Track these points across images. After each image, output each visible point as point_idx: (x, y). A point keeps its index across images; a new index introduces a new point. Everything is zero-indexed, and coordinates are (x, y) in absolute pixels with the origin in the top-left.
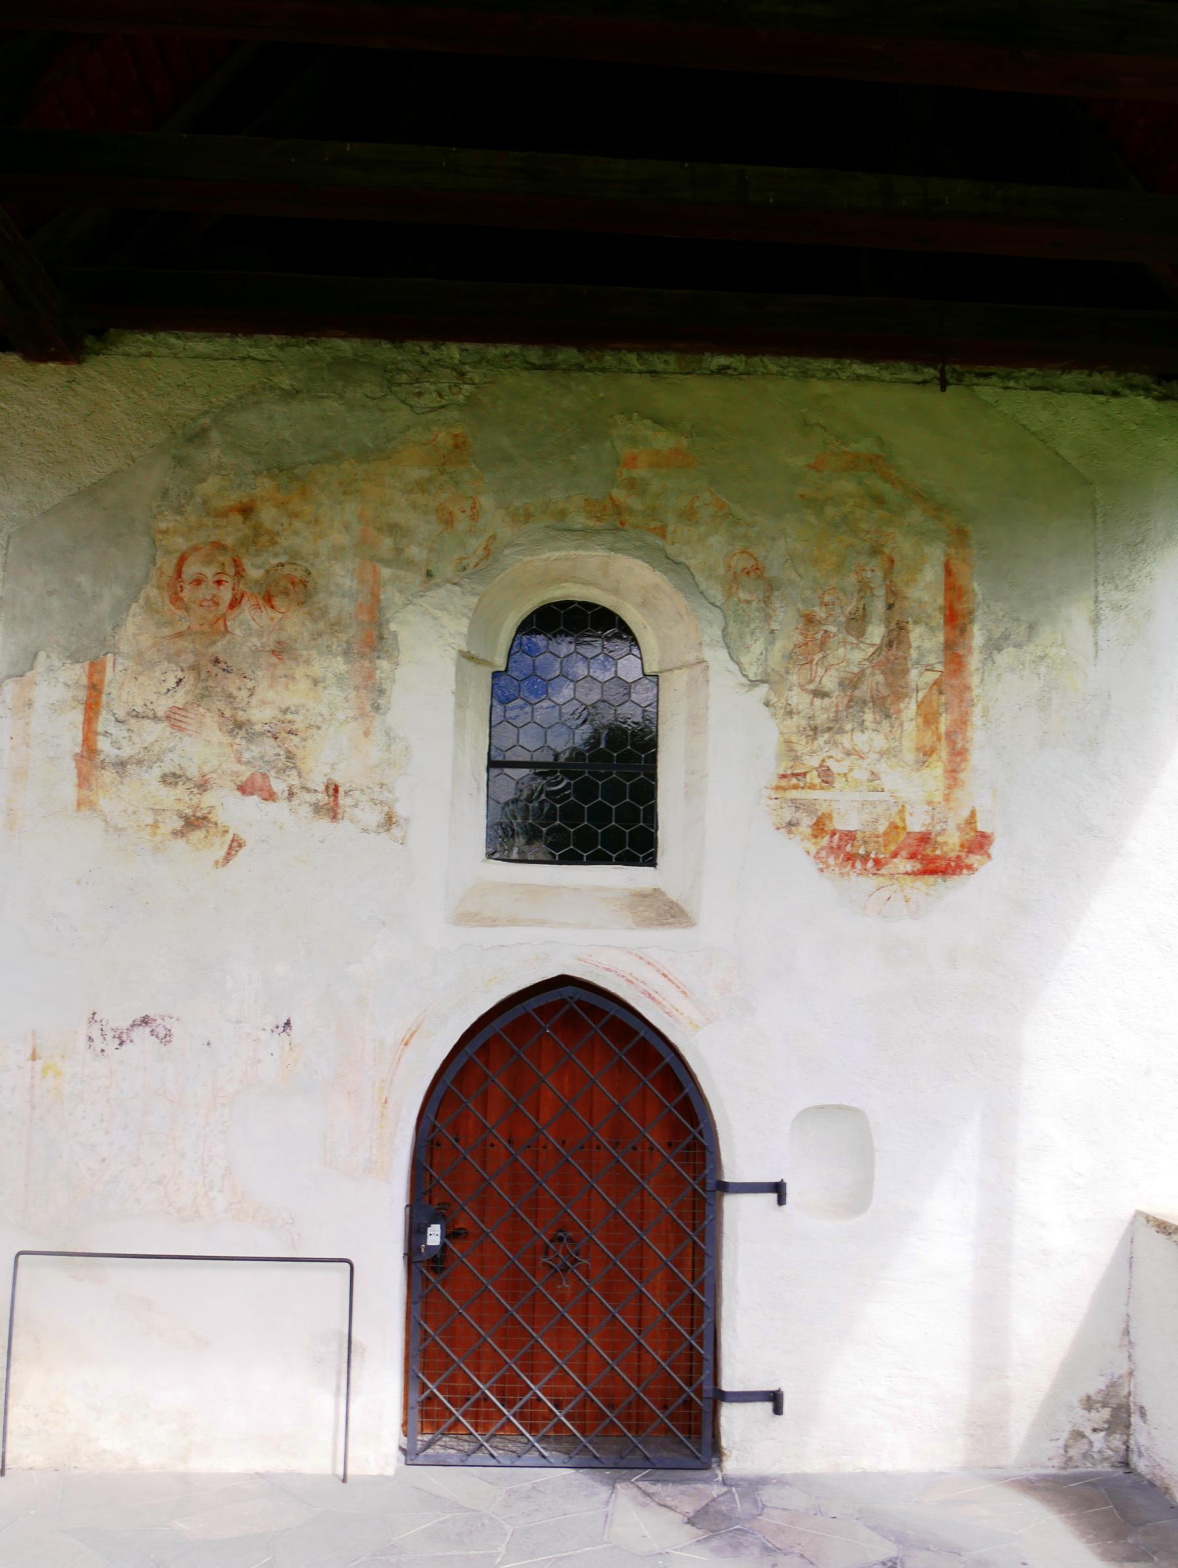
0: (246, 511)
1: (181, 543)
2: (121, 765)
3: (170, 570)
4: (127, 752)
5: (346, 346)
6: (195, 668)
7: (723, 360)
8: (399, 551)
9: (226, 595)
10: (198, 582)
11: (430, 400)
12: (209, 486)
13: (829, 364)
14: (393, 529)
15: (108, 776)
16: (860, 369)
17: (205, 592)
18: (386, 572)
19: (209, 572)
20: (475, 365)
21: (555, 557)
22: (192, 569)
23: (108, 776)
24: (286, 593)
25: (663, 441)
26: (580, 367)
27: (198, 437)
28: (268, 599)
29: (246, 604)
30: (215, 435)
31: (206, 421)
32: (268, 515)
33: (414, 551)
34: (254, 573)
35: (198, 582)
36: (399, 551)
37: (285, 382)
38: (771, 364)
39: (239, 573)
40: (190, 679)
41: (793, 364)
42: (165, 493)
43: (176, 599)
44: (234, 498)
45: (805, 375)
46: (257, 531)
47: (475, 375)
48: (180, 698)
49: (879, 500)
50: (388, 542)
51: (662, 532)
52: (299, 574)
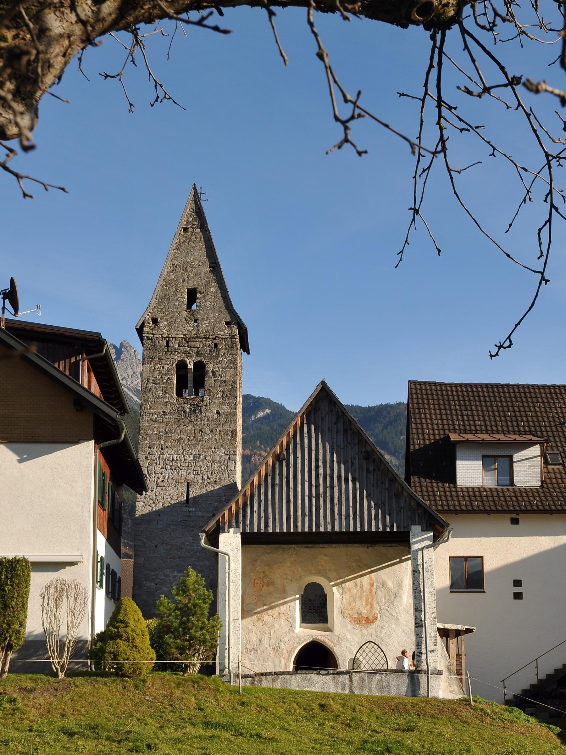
0: (264, 572)
1: (254, 577)
2: (248, 611)
3: (253, 582)
4: (248, 609)
5: (277, 545)
6: (257, 596)
7: (335, 545)
8: (287, 577)
9: (261, 585)
10: (257, 583)
11: (290, 553)
12: (258, 568)
13: (351, 545)
14: (286, 574)
15: (246, 613)
16: (356, 545)
17: (258, 585)
18: (285, 581)
19: (259, 582)
20: (297, 547)
21: (354, 461)
22: (256, 581)
23: (246, 613)
24: (270, 584)
25: (326, 558)
26: (313, 547)
27: (256, 561)
28: (268, 585)
29: (265, 586)
30: (258, 560)
31: (257, 558)
32: (267, 572)
33: (289, 577)
34: (266, 582)
35: (257, 583)
36: (287, 577)
37: (268, 551)
38: (342, 545)
39: (263, 582)
40: (257, 598)
41: (345, 545)
42: (251, 570)
43: (254, 586)
44: (262, 570)
45: (347, 547)
46: (265, 575)
47: (297, 549)
48: (256, 601)
49: (359, 566)
50: (285, 576)
51: (326, 573)
52: (272, 581)
